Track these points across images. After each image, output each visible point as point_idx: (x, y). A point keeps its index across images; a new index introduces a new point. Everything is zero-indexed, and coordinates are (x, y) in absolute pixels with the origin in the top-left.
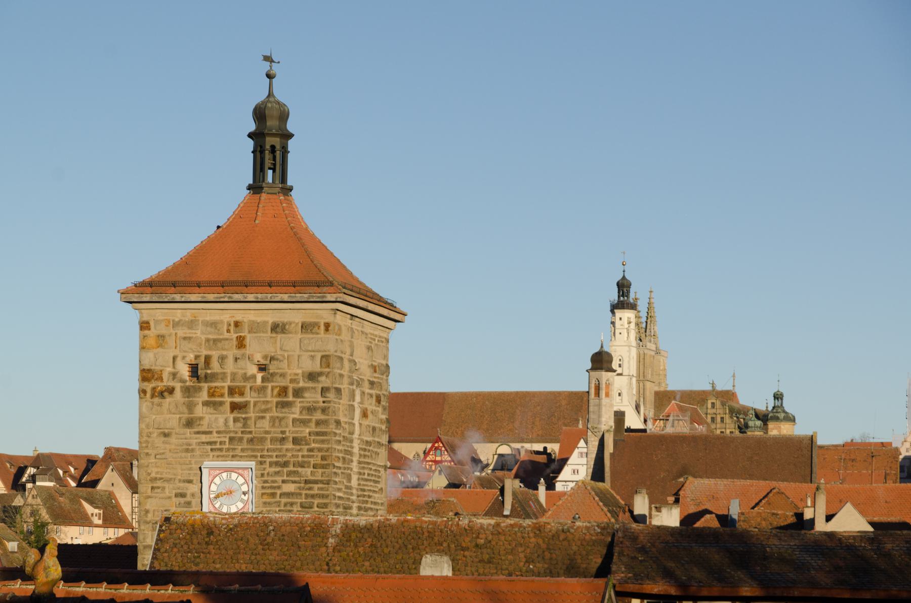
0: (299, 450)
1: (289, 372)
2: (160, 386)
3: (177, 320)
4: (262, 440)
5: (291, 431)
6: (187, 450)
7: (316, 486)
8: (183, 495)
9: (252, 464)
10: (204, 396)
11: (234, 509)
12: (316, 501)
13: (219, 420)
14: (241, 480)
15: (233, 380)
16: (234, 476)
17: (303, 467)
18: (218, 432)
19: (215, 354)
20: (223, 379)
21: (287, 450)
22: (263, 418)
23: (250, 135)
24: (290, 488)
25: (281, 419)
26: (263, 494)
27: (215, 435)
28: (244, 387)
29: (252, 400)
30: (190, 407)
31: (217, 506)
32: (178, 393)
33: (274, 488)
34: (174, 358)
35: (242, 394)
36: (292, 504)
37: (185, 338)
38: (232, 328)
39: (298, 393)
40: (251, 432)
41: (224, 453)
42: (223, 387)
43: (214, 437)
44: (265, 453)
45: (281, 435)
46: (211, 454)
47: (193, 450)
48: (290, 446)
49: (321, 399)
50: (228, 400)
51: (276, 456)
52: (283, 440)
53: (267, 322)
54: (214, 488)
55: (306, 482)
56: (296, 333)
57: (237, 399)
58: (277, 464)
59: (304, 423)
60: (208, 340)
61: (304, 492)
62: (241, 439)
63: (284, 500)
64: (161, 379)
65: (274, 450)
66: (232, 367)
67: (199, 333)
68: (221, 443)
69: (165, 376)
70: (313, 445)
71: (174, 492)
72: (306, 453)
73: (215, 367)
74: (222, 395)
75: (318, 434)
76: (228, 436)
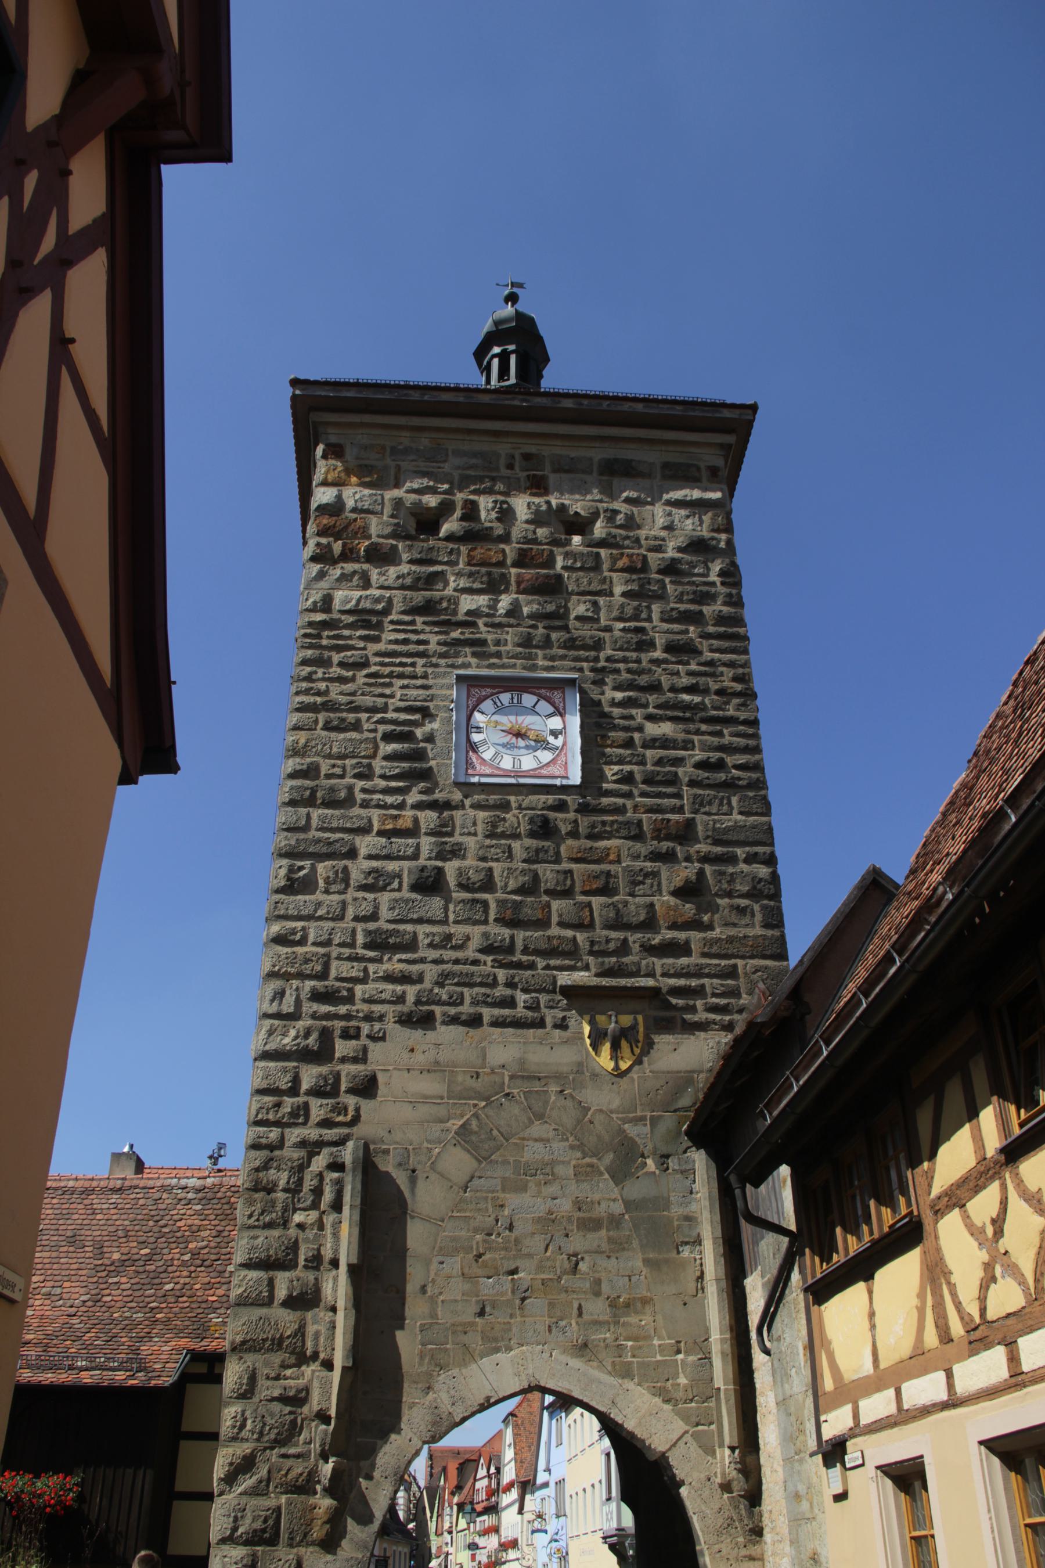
0: (679, 663)
3: (400, 447)
8: (408, 737)
11: (528, 763)
12: (730, 760)
14: (544, 707)
16: (528, 699)
17: (691, 689)
18: (486, 625)
27: (483, 628)
31: (487, 755)
33: (626, 729)
39: (671, 569)
51: (629, 671)
56: (649, 475)
61: (696, 738)
63: (649, 753)
65: (625, 660)
70: (708, 655)
71: (382, 728)
72: (693, 667)
76: (510, 629)
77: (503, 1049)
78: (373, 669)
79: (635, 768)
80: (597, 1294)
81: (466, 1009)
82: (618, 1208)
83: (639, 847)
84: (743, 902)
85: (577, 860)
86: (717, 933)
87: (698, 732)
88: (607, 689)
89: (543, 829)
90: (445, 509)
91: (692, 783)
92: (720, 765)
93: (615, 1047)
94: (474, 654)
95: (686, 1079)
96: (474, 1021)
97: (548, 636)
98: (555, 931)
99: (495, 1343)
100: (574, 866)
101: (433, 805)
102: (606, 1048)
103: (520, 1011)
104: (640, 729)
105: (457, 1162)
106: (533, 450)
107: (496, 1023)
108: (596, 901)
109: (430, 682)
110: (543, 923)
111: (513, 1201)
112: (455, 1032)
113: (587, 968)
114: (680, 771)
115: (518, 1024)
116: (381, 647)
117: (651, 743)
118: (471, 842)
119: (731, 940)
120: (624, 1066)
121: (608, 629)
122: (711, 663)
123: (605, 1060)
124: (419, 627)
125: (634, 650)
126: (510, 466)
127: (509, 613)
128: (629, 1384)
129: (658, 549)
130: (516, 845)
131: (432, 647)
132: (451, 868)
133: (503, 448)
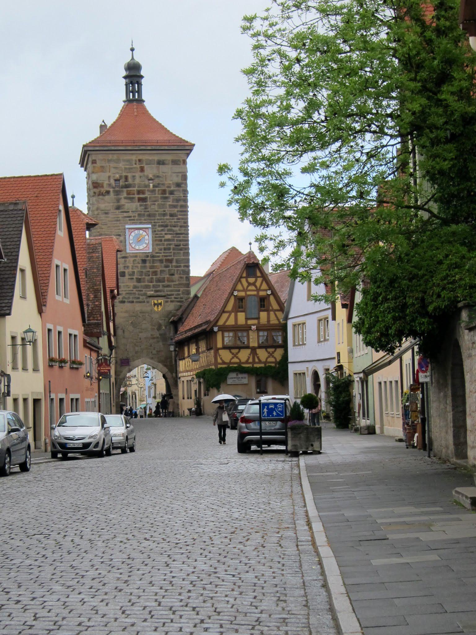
1: (166, 182)
2: (103, 190)
4: (154, 215)
5: (168, 210)
6: (117, 221)
7: (181, 236)
9: (150, 226)
10: (125, 195)
11: (141, 247)
12: (182, 243)
13: (133, 206)
14: (144, 233)
15: (139, 187)
16: (141, 232)
17: (175, 227)
18: (132, 212)
19: (130, 175)
20: (134, 187)
21: (167, 219)
22: (154, 204)
23: (125, 77)
24: (169, 237)
25: (163, 205)
26: (156, 240)
27: (131, 213)
29: (149, 196)
30: (118, 200)
31: (133, 246)
32: (112, 194)
34: (109, 177)
36: (170, 245)
37: (114, 168)
38: (137, 162)
39: (172, 193)
40: (148, 211)
41: (135, 221)
42: (134, 190)
43: (130, 214)
44: (156, 221)
46: (129, 222)
47: (119, 220)
48: (168, 217)
49: (182, 195)
50: (137, 196)
52: (164, 215)
53: (154, 160)
54: (131, 237)
55: (177, 234)
56: (168, 164)
57: (141, 196)
58: (162, 226)
59: (175, 207)
60: (126, 168)
62: (144, 215)
63: (166, 243)
64: (103, 187)
65: (161, 219)
66: (138, 180)
67: (121, 165)
68: (134, 216)
69: (105, 185)
72: (176, 220)
73: (130, 181)
74: (134, 194)
75: (181, 211)
77: (138, 307)
78: (109, 225)
79: (163, 247)
80: (154, 349)
81: (131, 300)
82: (158, 336)
83: (163, 265)
85: (150, 269)
86: (177, 283)
87: (176, 237)
88: (157, 227)
89: (144, 261)
90: (121, 177)
91: (174, 249)
92: (180, 245)
93: (158, 306)
94: (130, 220)
95: (170, 312)
96: (133, 302)
97: (144, 215)
98: (147, 283)
99: (138, 358)
100: (151, 270)
102: (156, 306)
103: (140, 300)
104: (163, 237)
105: (131, 328)
106: (140, 157)
107: (137, 302)
108: (154, 277)
109: (121, 228)
110: (144, 282)
111: (140, 334)
112: (129, 304)
113: (152, 291)
114: (172, 247)
115: (140, 302)
116: (109, 219)
117: (166, 240)
118: (130, 265)
119: (180, 284)
120: (159, 310)
121: (157, 211)
122: (178, 219)
123: (156, 308)
126: (136, 164)
127: (137, 209)
128: (160, 364)
129: (169, 187)
130: (139, 265)
131: (120, 218)
132: (126, 271)
133: (134, 158)
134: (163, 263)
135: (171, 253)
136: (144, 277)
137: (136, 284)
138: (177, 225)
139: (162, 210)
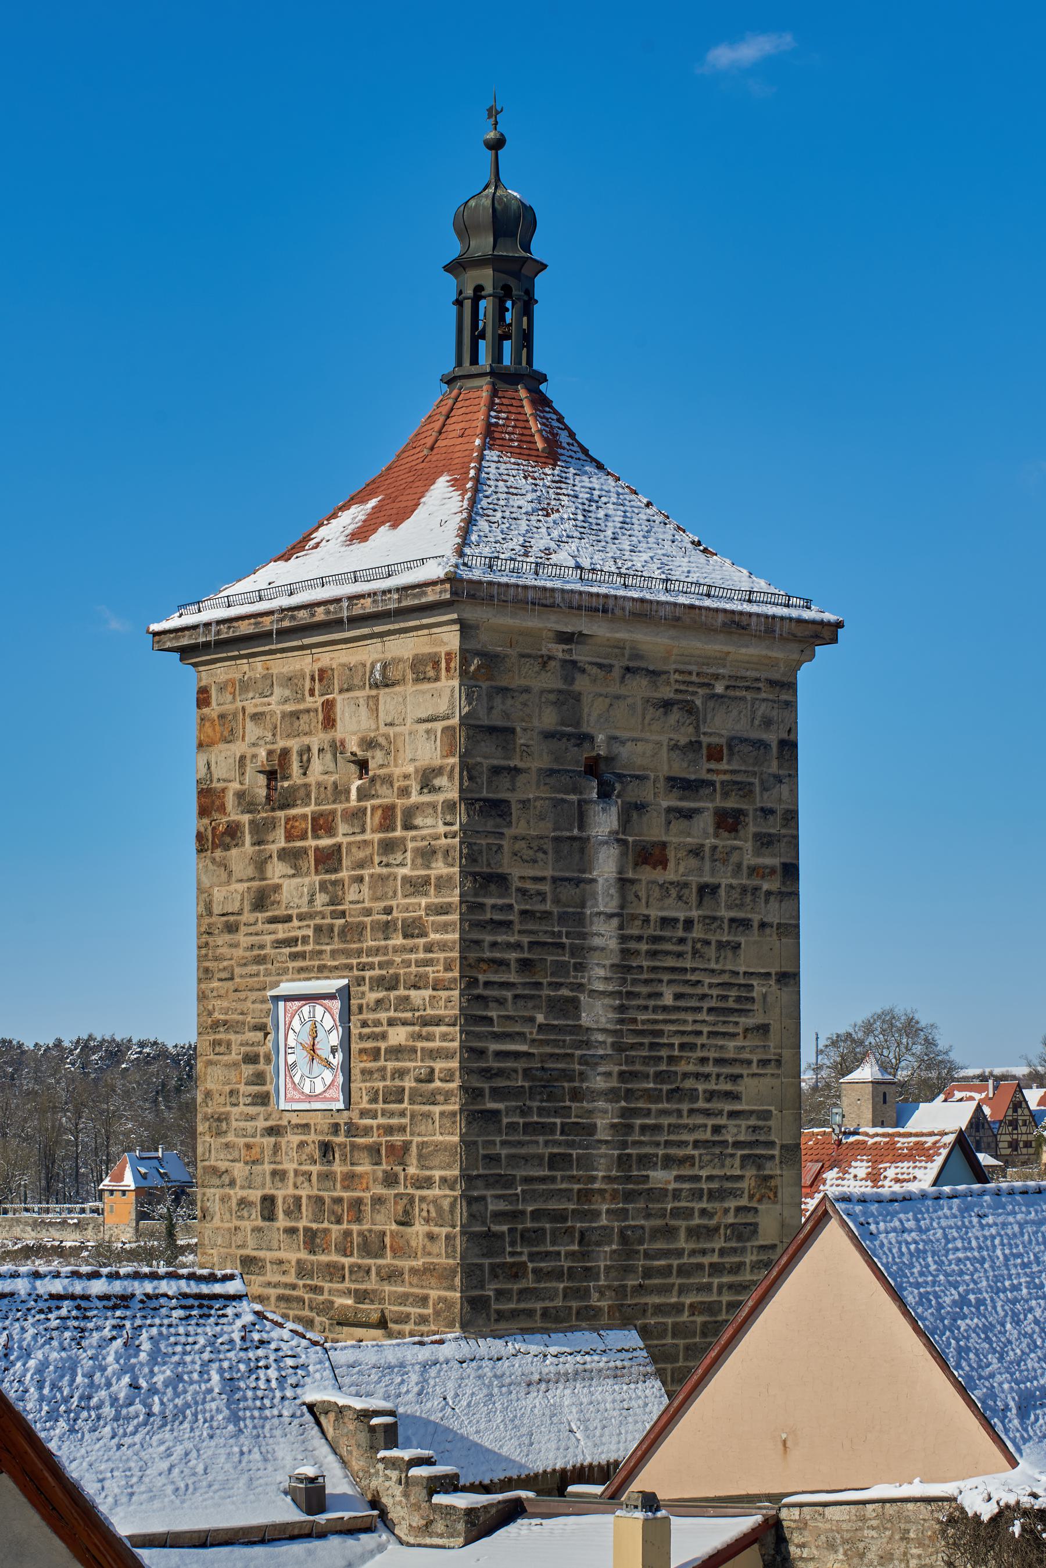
20: (306, 801)
24: (398, 1036)
26: (362, 1051)
28: (333, 813)
35: (331, 831)
36: (401, 1073)
45: (384, 917)
46: (291, 965)
70: (434, 936)
76: (312, 923)
84: (436, 1230)
97: (331, 928)
101: (272, 1131)
104: (384, 1036)
108: (355, 1227)
114: (408, 1083)
116: (239, 952)
124: (260, 926)
125: (385, 939)
134: (378, 1163)
135: (402, 1114)
136: (326, 1225)
137: (303, 1255)
138: (426, 975)
139: (383, 904)
